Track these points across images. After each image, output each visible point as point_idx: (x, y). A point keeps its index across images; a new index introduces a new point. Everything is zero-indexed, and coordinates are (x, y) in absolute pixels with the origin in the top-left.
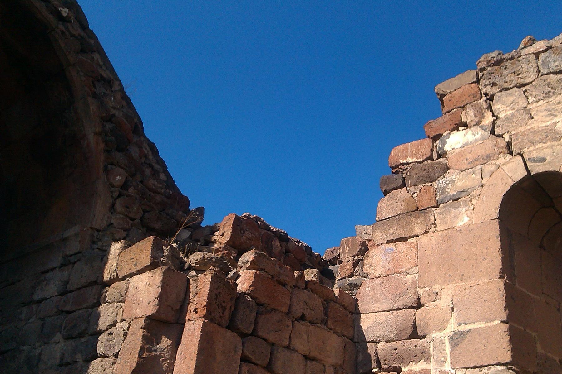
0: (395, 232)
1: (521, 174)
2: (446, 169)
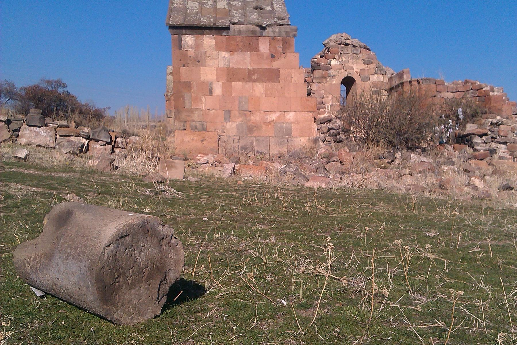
0: (319, 81)
1: (346, 76)
2: (330, 69)
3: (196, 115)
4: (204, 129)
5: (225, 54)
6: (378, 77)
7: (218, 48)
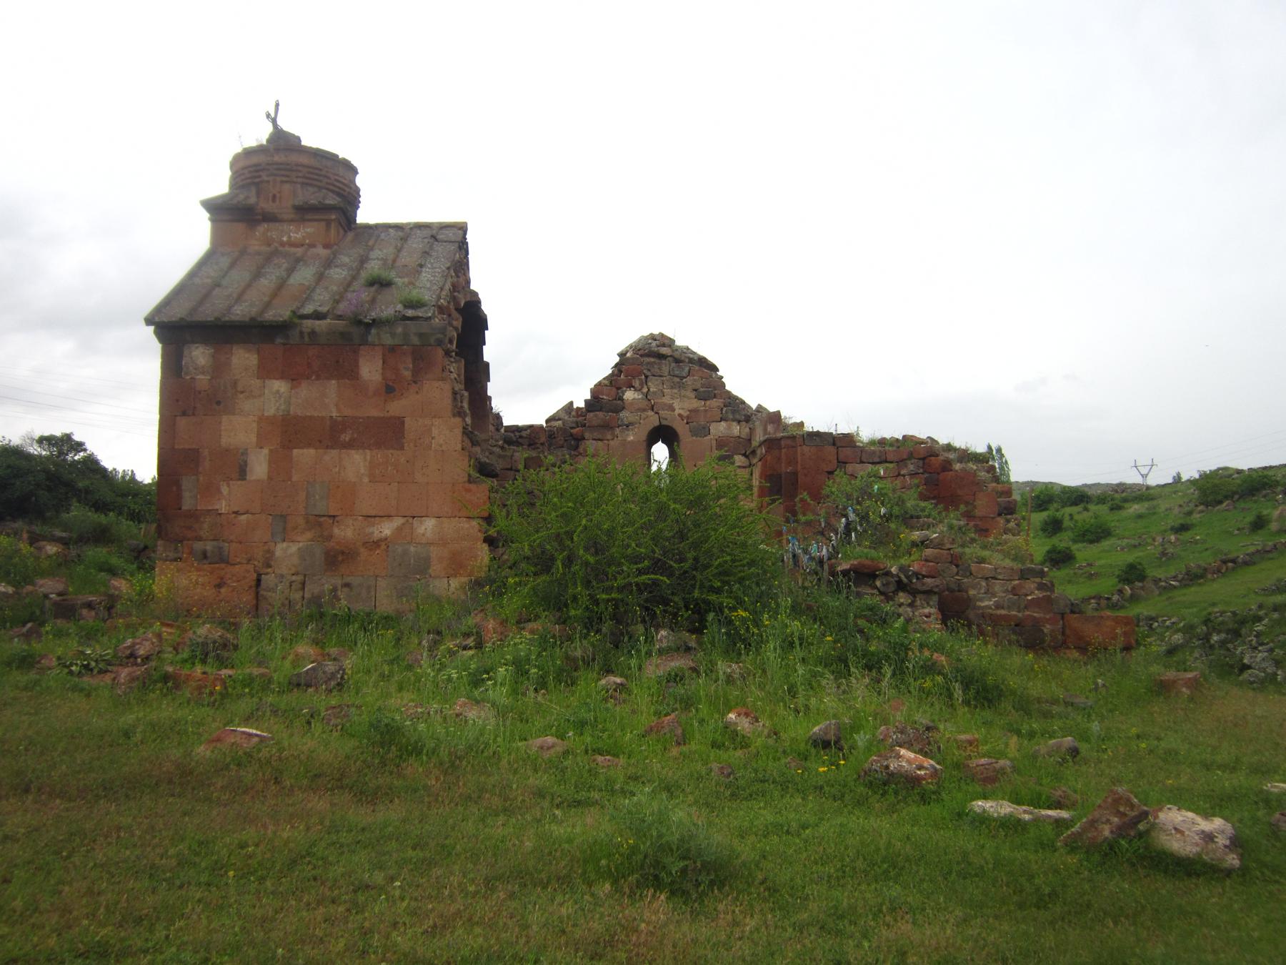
0: (596, 435)
1: (657, 423)
2: (624, 408)
3: (206, 526)
4: (222, 559)
5: (280, 386)
6: (729, 428)
7: (265, 372)
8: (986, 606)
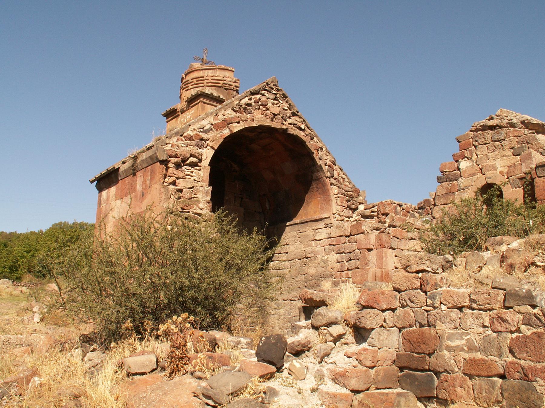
8: (458, 346)
